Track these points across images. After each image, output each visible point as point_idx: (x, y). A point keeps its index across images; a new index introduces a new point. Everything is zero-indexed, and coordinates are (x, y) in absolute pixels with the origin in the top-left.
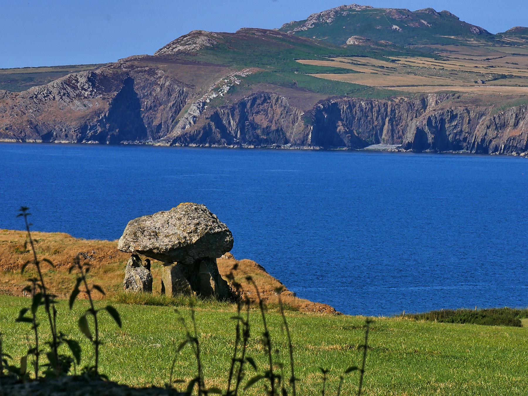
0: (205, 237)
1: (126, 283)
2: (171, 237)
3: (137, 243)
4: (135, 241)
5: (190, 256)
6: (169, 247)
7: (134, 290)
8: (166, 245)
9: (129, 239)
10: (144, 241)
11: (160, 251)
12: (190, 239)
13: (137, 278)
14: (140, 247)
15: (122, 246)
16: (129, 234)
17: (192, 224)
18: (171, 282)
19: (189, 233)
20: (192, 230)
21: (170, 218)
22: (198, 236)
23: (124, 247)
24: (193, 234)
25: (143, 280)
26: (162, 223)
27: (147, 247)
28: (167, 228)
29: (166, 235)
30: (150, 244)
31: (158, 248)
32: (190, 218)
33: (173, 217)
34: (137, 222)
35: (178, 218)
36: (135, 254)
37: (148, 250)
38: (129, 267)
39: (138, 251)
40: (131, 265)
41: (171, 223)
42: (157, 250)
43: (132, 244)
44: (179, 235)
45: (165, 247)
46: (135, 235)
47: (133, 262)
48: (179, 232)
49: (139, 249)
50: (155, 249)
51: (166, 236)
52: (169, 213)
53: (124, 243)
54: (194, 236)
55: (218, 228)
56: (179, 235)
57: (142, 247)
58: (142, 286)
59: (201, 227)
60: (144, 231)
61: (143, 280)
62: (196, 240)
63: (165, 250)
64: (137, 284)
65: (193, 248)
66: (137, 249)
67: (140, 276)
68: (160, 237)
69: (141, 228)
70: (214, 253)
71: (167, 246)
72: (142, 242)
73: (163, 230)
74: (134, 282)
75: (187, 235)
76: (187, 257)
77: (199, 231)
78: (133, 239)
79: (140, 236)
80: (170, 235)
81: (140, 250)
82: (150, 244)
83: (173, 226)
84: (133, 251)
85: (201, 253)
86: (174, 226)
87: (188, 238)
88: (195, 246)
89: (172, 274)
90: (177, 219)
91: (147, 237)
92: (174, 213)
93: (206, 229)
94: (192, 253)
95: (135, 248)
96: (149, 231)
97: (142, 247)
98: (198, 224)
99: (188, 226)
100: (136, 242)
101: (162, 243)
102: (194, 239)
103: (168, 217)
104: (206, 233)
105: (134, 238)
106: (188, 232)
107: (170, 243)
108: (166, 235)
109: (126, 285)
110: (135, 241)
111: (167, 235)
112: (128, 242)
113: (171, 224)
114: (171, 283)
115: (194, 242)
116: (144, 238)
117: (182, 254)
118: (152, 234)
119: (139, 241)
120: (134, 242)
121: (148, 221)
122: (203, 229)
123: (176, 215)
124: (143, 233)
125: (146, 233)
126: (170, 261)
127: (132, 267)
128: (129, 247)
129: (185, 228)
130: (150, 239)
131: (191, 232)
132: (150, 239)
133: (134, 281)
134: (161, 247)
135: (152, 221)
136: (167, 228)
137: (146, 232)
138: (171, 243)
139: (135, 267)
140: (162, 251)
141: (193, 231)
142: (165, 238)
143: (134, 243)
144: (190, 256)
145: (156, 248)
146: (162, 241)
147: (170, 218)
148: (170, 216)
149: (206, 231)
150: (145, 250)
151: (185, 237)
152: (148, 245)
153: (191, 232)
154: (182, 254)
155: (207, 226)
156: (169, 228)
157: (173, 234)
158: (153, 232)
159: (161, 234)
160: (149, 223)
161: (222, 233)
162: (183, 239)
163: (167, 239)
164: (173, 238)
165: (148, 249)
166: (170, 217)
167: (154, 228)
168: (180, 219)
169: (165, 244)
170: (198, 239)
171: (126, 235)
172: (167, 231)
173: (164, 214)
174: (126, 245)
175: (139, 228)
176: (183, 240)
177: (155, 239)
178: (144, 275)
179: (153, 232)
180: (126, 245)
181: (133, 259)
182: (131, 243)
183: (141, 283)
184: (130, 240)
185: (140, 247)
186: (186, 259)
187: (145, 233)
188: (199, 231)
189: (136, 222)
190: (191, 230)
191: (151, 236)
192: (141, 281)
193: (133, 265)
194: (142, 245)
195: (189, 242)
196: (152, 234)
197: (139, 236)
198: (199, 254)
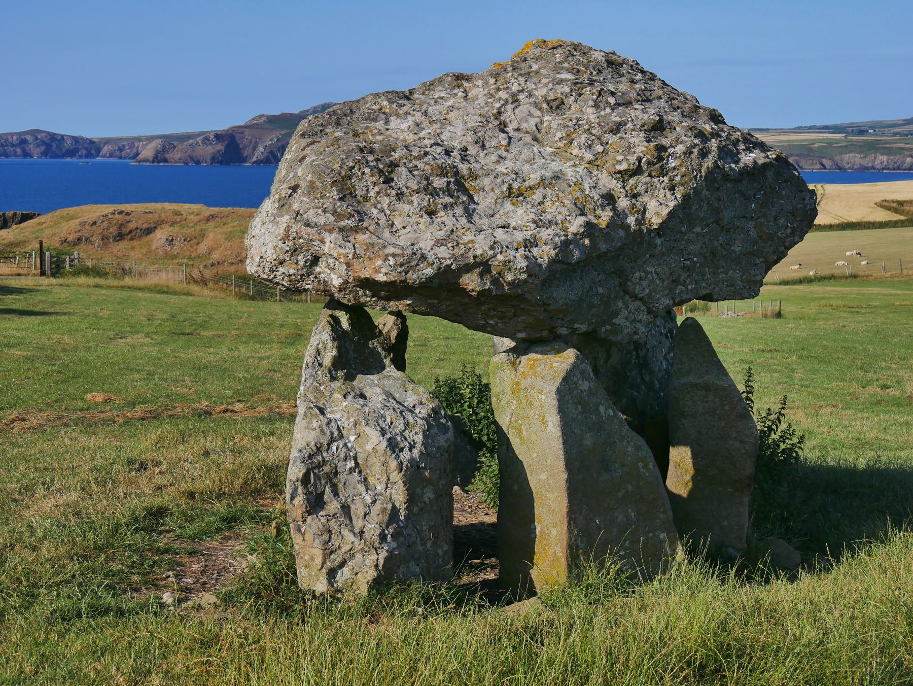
0: (705, 192)
1: (305, 480)
2: (537, 196)
3: (361, 237)
4: (351, 223)
5: (635, 297)
6: (545, 254)
7: (358, 524)
8: (529, 244)
9: (311, 215)
10: (398, 225)
11: (495, 281)
12: (633, 206)
13: (369, 448)
14: (379, 262)
15: (270, 255)
16: (312, 186)
17: (629, 125)
18: (561, 454)
19: (623, 176)
20: (639, 160)
21: (506, 102)
22: (672, 189)
23: (281, 263)
24: (644, 179)
25: (406, 456)
26: (471, 124)
27: (424, 257)
28: (502, 152)
29: (510, 188)
30: (439, 243)
31: (483, 266)
32: (612, 100)
33: (521, 97)
34: (345, 120)
35: (548, 102)
36: (347, 299)
37: (430, 279)
38: (314, 377)
39: (367, 284)
40: (327, 360)
41: (514, 125)
42: (481, 275)
43: (330, 244)
44: (578, 184)
45: (526, 257)
46: (347, 194)
47: (339, 348)
48: (569, 172)
49: (377, 271)
50: (468, 268)
51: (515, 195)
52: (492, 81)
53: (285, 238)
54: (650, 189)
55: (748, 150)
56: (578, 184)
57: (392, 261)
58: (399, 495)
59: (678, 141)
60: (393, 165)
61: (406, 456)
62: (665, 212)
63: (524, 276)
64: (372, 480)
65: (652, 256)
66: (365, 274)
67: (383, 432)
68: (484, 202)
69: (372, 152)
70: (738, 274)
71: (535, 251)
72: (387, 234)
73: (488, 160)
74: (351, 471)
75: (614, 185)
76: (620, 304)
77: (672, 163)
78: (335, 213)
79: (372, 193)
80: (531, 188)
81: (381, 278)
82: (439, 243)
83: (528, 139)
84: (336, 281)
85: (684, 275)
86: (535, 139)
87: (623, 203)
88: (658, 241)
89: (562, 410)
90: (545, 106)
91: (416, 199)
92: (522, 80)
93: (704, 154)
94: (645, 283)
95: (348, 265)
96: (421, 165)
97: (392, 261)
98: (659, 127)
99: (612, 139)
100: (356, 230)
101: (500, 234)
102: (652, 205)
103: (492, 96)
104: (710, 172)
105: (342, 207)
106: (623, 167)
107: (545, 234)
108: (510, 188)
109: (308, 494)
110: (351, 223)
111: (516, 185)
112: (304, 232)
113: (518, 130)
114: (561, 464)
115: (656, 221)
116: (400, 206)
117: (601, 290)
118: (439, 182)
119: (372, 228)
120: (342, 230)
121: (398, 115)
122: (688, 153)
123: (530, 86)
124: (388, 181)
125: (402, 177)
126: (545, 333)
127: (333, 378)
128: (315, 260)
129: (600, 149)
130: (431, 213)
131: (637, 171)
132: (431, 213)
133: (351, 464)
134: (500, 257)
135: (418, 117)
136: (502, 152)
137: (402, 170)
138: (549, 231)
139: (350, 377)
140: (510, 277)
141: (650, 163)
142: (508, 206)
143: (346, 239)
144: (635, 297)
145: (476, 265)
146: (498, 221)
147: (506, 102)
148: (503, 94)
149: (709, 162)
150: (412, 277)
151: (609, 199)
152: (425, 245)
153: (637, 171)
154: (601, 290)
155: (700, 134)
156: (514, 149)
157: (543, 183)
158: (442, 171)
159: (486, 181)
160: (404, 126)
161: (770, 174)
162: (603, 207)
163: (520, 211)
164: (548, 203)
165: (429, 271)
166: (503, 94)
167: (439, 150)
168: (557, 106)
169: (519, 236)
170: (672, 204)
171: (295, 188)
172: (509, 164)
173: (466, 84)
174: (295, 251)
175: (361, 150)
176: (605, 217)
177: (459, 210)
178: (407, 425)
179: (442, 171)
180: (295, 251)
181: (335, 322)
182: (328, 237)
183: (396, 476)
184: (321, 220)
185: (379, 262)
186: (616, 314)
187: (400, 177)
188: (672, 163)
189: (338, 124)
190: (633, 159)
191: (434, 193)
192: (394, 464)
193: (337, 363)
194: (390, 250)
195: (631, 220)
196: (439, 182)
197: (366, 199)
198: (676, 282)
